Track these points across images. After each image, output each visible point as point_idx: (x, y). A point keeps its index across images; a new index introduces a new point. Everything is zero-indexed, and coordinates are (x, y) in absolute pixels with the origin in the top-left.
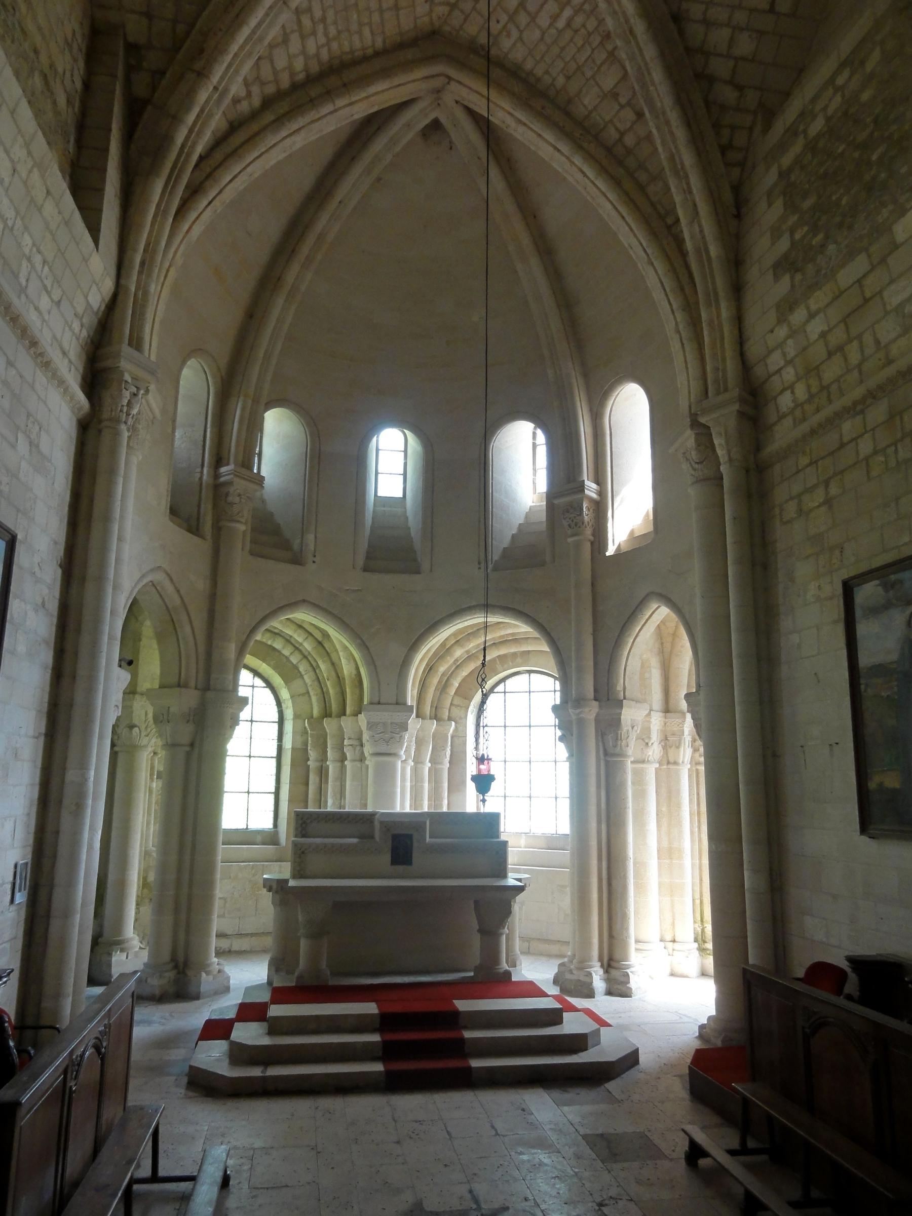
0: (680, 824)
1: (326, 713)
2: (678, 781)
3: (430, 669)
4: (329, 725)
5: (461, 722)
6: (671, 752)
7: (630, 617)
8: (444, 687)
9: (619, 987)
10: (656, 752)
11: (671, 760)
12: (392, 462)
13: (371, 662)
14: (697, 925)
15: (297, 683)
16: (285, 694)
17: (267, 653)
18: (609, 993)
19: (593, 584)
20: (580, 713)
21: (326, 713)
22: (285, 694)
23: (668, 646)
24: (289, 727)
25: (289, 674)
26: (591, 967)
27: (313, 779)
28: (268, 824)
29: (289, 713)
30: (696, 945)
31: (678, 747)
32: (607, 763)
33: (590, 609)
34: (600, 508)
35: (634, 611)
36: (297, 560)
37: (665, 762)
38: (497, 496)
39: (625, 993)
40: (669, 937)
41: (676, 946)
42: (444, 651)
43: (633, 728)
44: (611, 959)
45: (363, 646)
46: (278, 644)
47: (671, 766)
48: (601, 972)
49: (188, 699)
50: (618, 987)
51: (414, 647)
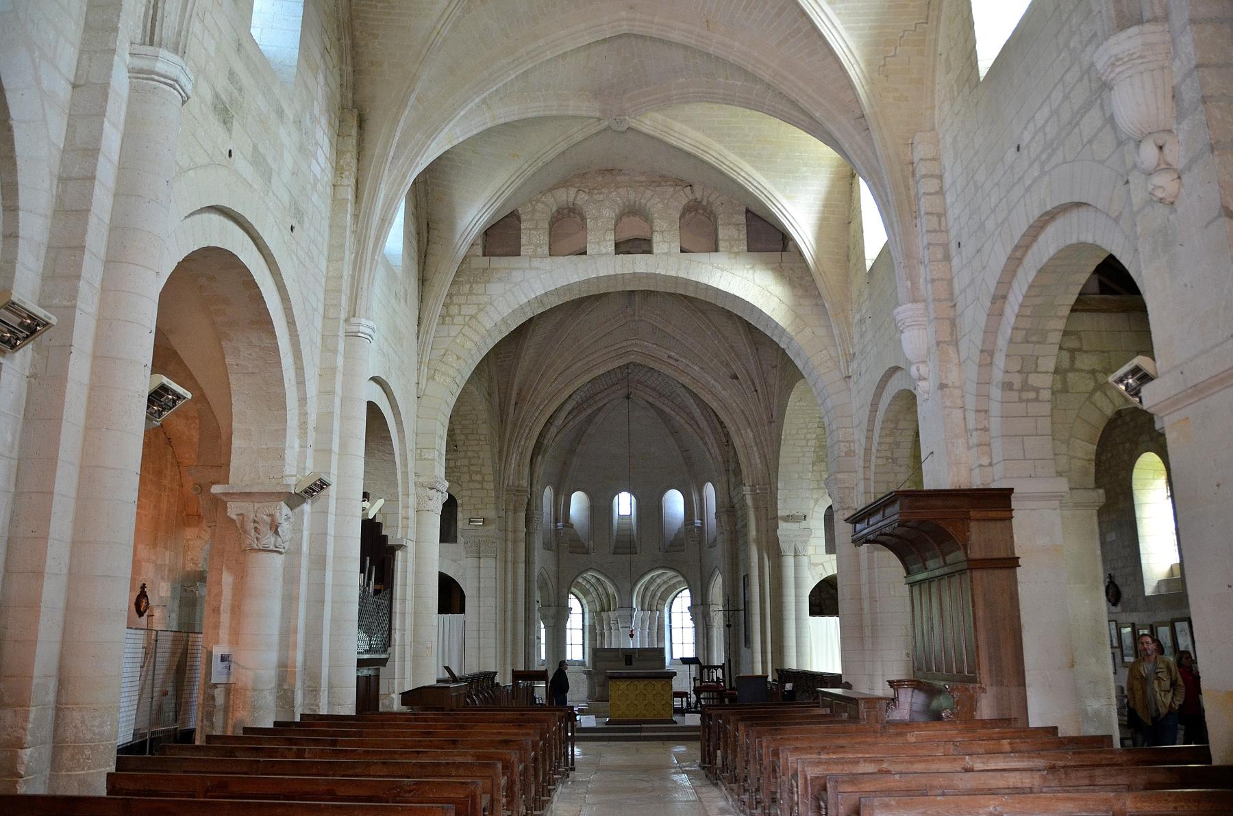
1: (603, 610)
3: (646, 589)
4: (604, 615)
5: (662, 612)
7: (711, 575)
8: (653, 596)
12: (625, 504)
13: (618, 590)
15: (589, 597)
16: (584, 601)
17: (578, 586)
21: (603, 610)
22: (584, 601)
24: (587, 616)
25: (586, 593)
27: (598, 638)
28: (580, 658)
29: (587, 610)
34: (701, 529)
36: (587, 553)
38: (667, 519)
42: (652, 580)
45: (615, 585)
46: (580, 580)
49: (553, 610)
51: (635, 584)
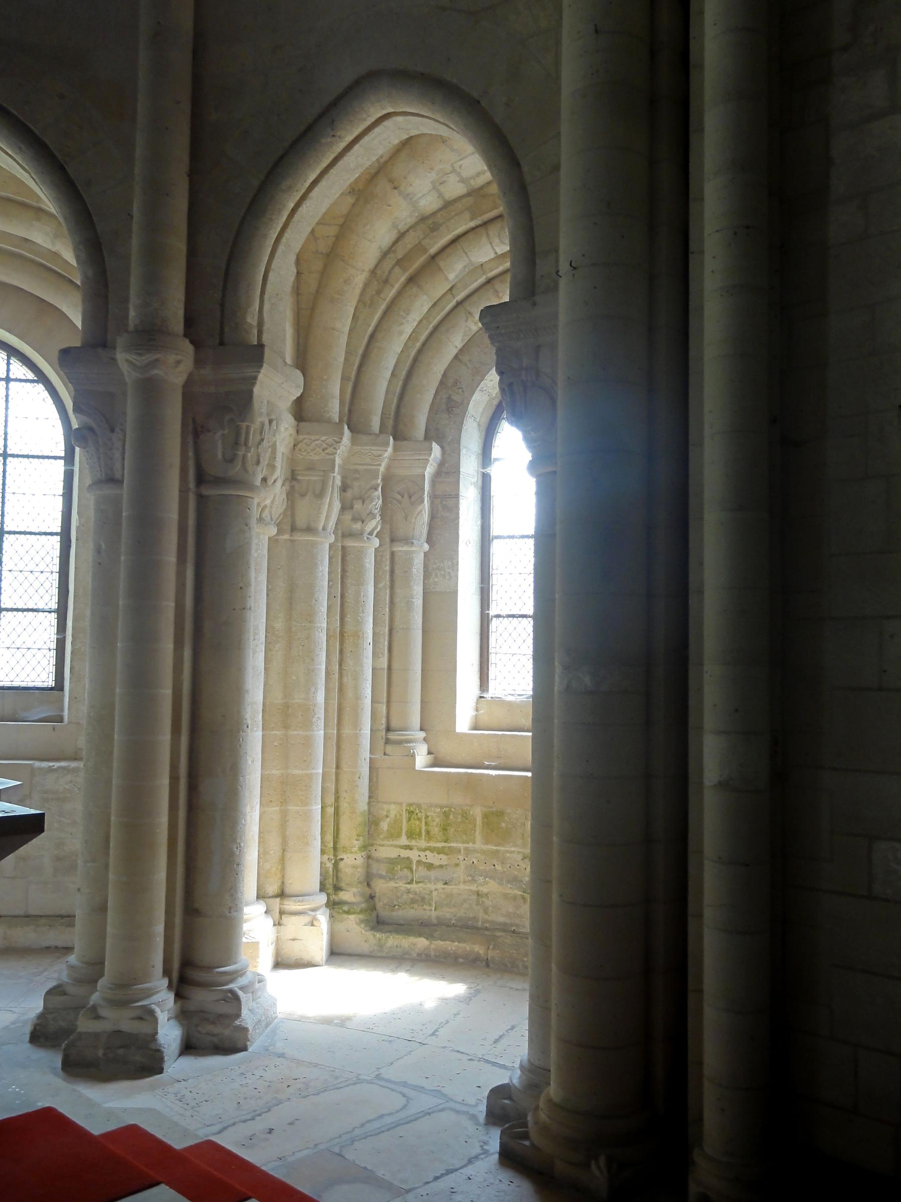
0: (310, 655)
2: (312, 566)
6: (303, 507)
9: (211, 1028)
10: (277, 498)
11: (301, 522)
14: (326, 857)
18: (189, 1048)
19: (195, 52)
20: (154, 363)
23: (312, 281)
26: (149, 993)
30: (323, 898)
31: (320, 495)
32: (201, 499)
33: (186, 107)
35: (310, 128)
37: (287, 527)
39: (230, 1045)
40: (272, 888)
41: (291, 905)
43: (271, 422)
44: (187, 963)
47: (300, 537)
48: (170, 997)
50: (215, 1031)
